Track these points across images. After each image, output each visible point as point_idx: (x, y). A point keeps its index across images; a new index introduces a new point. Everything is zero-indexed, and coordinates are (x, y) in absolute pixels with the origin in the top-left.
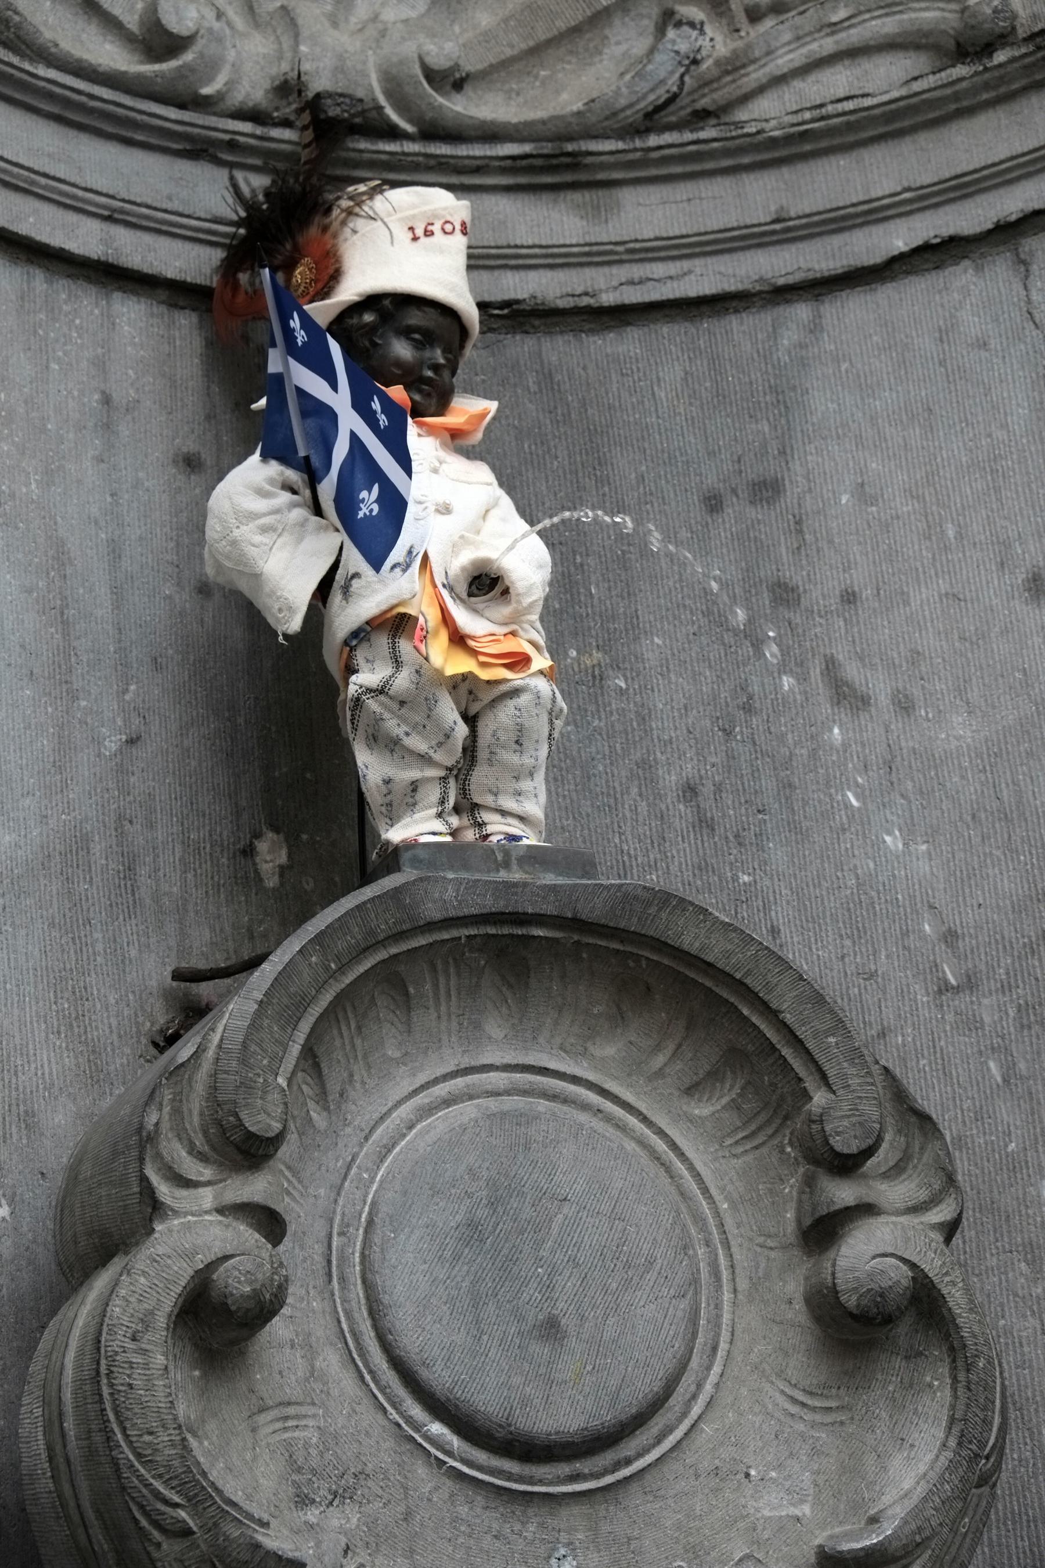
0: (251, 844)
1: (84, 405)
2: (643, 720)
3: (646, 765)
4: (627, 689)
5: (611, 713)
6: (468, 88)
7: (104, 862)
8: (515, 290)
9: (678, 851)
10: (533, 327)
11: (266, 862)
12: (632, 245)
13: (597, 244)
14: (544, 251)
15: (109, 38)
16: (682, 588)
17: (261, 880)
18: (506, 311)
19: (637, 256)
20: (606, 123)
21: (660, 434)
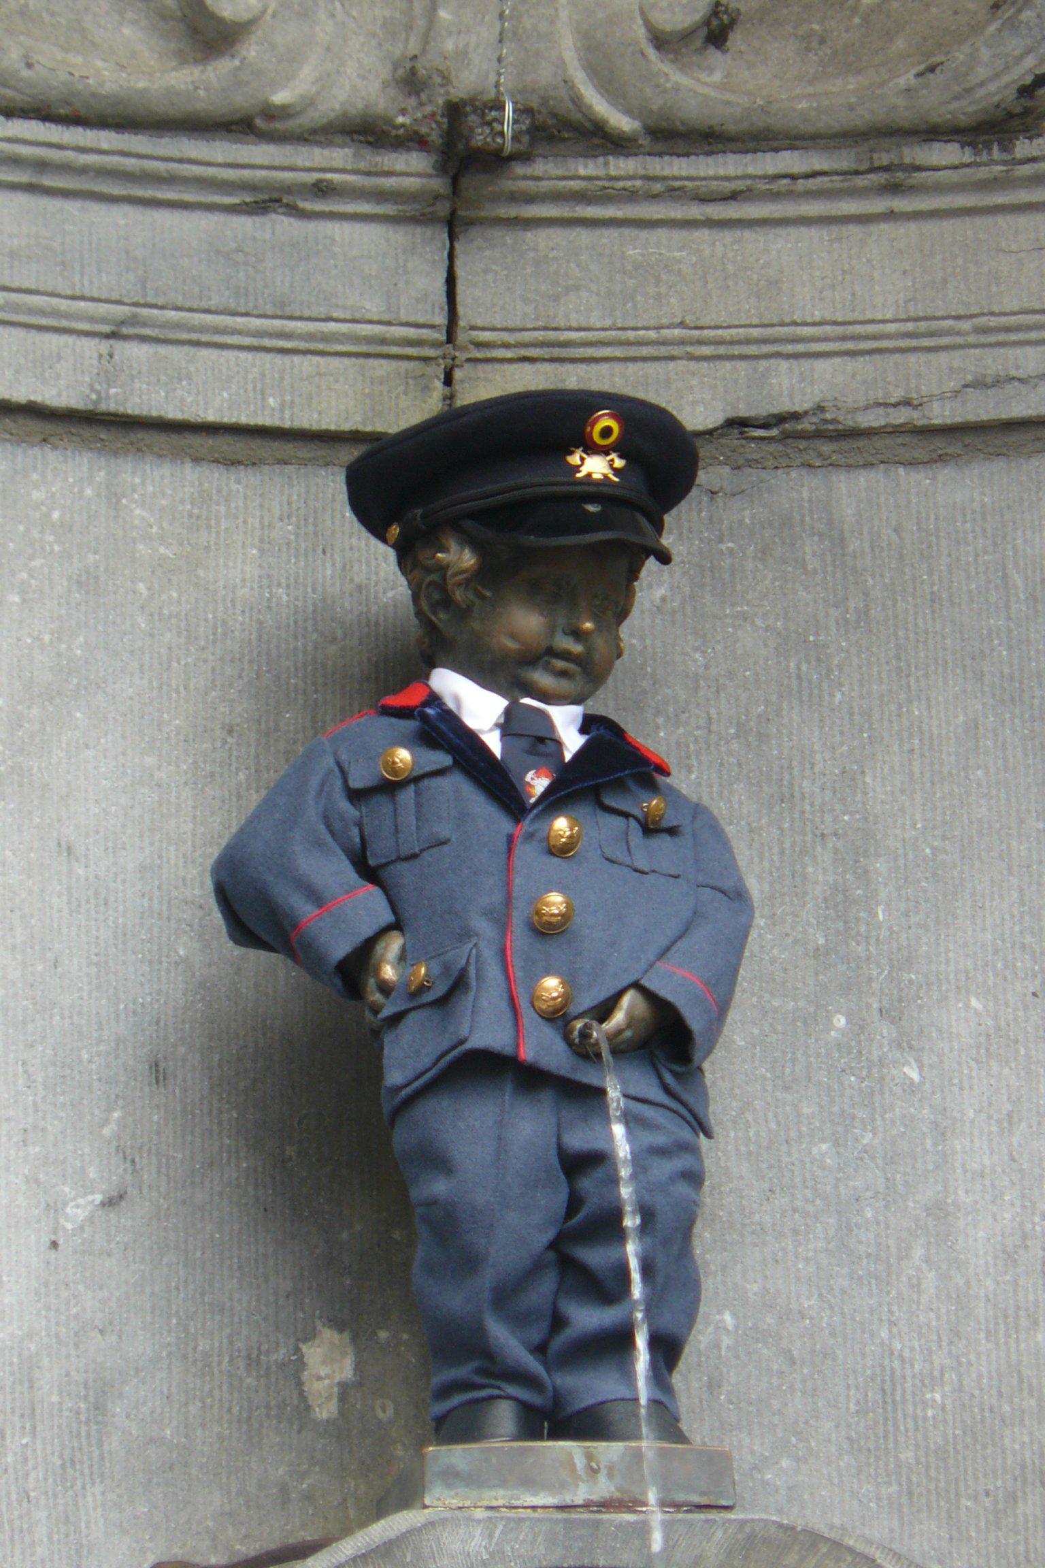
0: (297, 1350)
1: (59, 655)
2: (941, 1134)
3: (940, 1211)
4: (922, 1083)
5: (893, 1122)
6: (736, 39)
7: (55, 1399)
8: (791, 396)
9: (978, 1355)
10: (820, 455)
11: (319, 1378)
12: (982, 320)
13: (926, 319)
14: (840, 330)
15: (130, 15)
16: (1022, 914)
17: (308, 1408)
18: (774, 432)
19: (992, 339)
20: (955, 105)
21: (1010, 648)
